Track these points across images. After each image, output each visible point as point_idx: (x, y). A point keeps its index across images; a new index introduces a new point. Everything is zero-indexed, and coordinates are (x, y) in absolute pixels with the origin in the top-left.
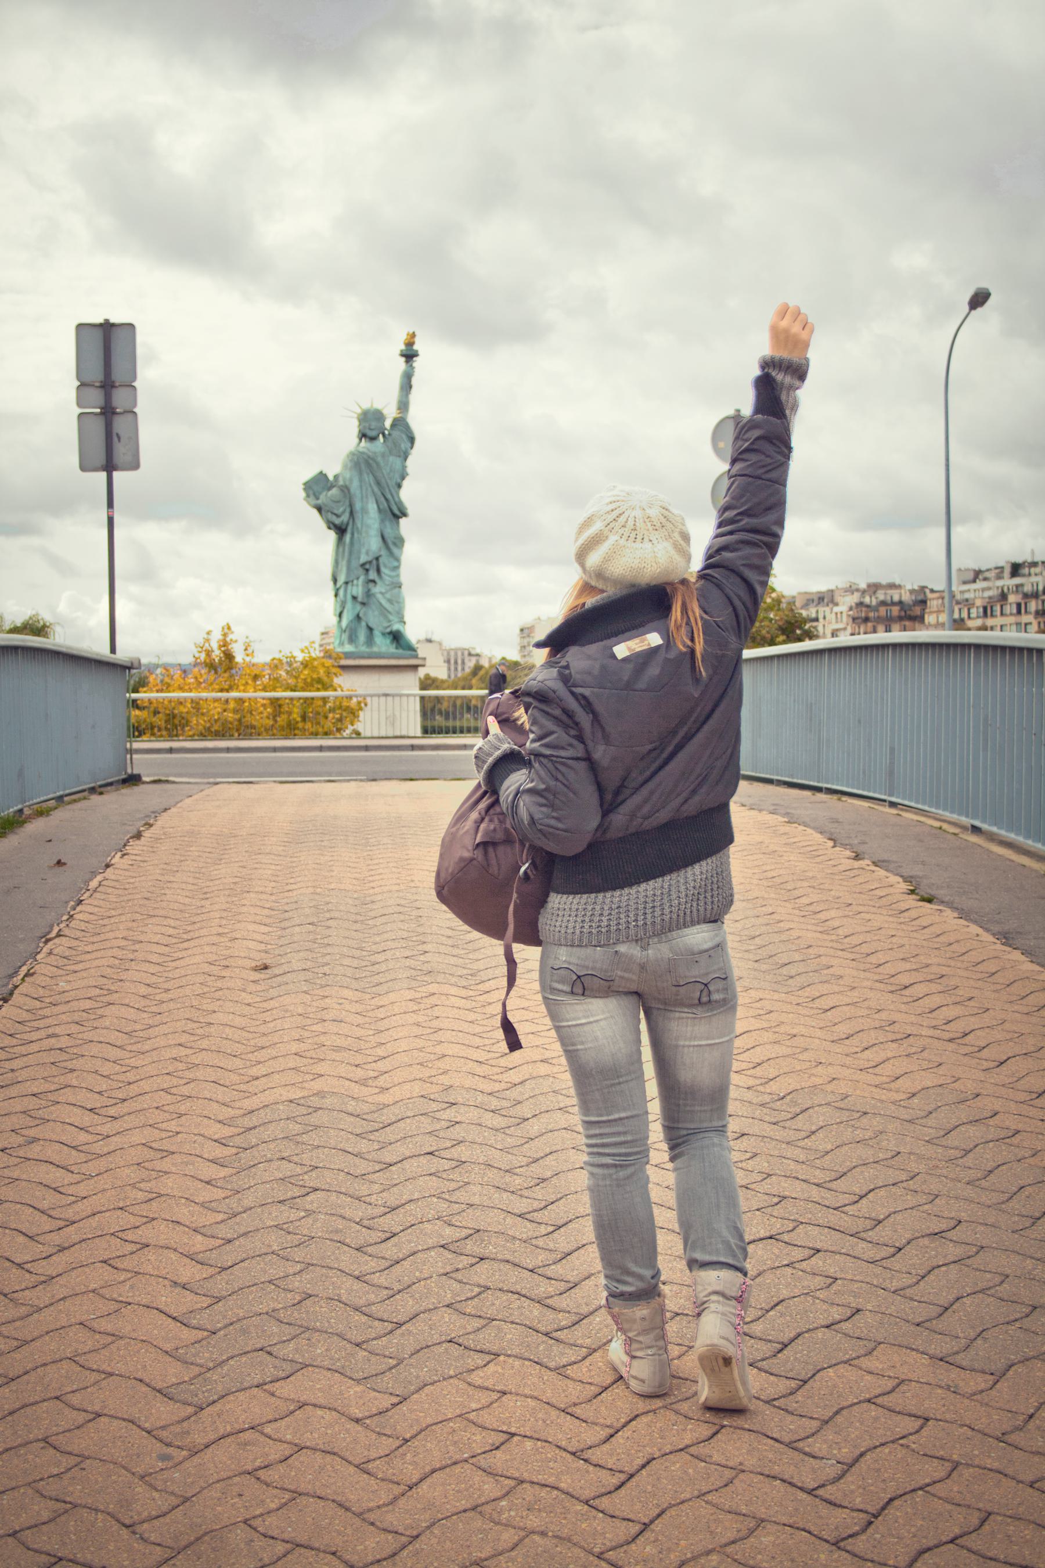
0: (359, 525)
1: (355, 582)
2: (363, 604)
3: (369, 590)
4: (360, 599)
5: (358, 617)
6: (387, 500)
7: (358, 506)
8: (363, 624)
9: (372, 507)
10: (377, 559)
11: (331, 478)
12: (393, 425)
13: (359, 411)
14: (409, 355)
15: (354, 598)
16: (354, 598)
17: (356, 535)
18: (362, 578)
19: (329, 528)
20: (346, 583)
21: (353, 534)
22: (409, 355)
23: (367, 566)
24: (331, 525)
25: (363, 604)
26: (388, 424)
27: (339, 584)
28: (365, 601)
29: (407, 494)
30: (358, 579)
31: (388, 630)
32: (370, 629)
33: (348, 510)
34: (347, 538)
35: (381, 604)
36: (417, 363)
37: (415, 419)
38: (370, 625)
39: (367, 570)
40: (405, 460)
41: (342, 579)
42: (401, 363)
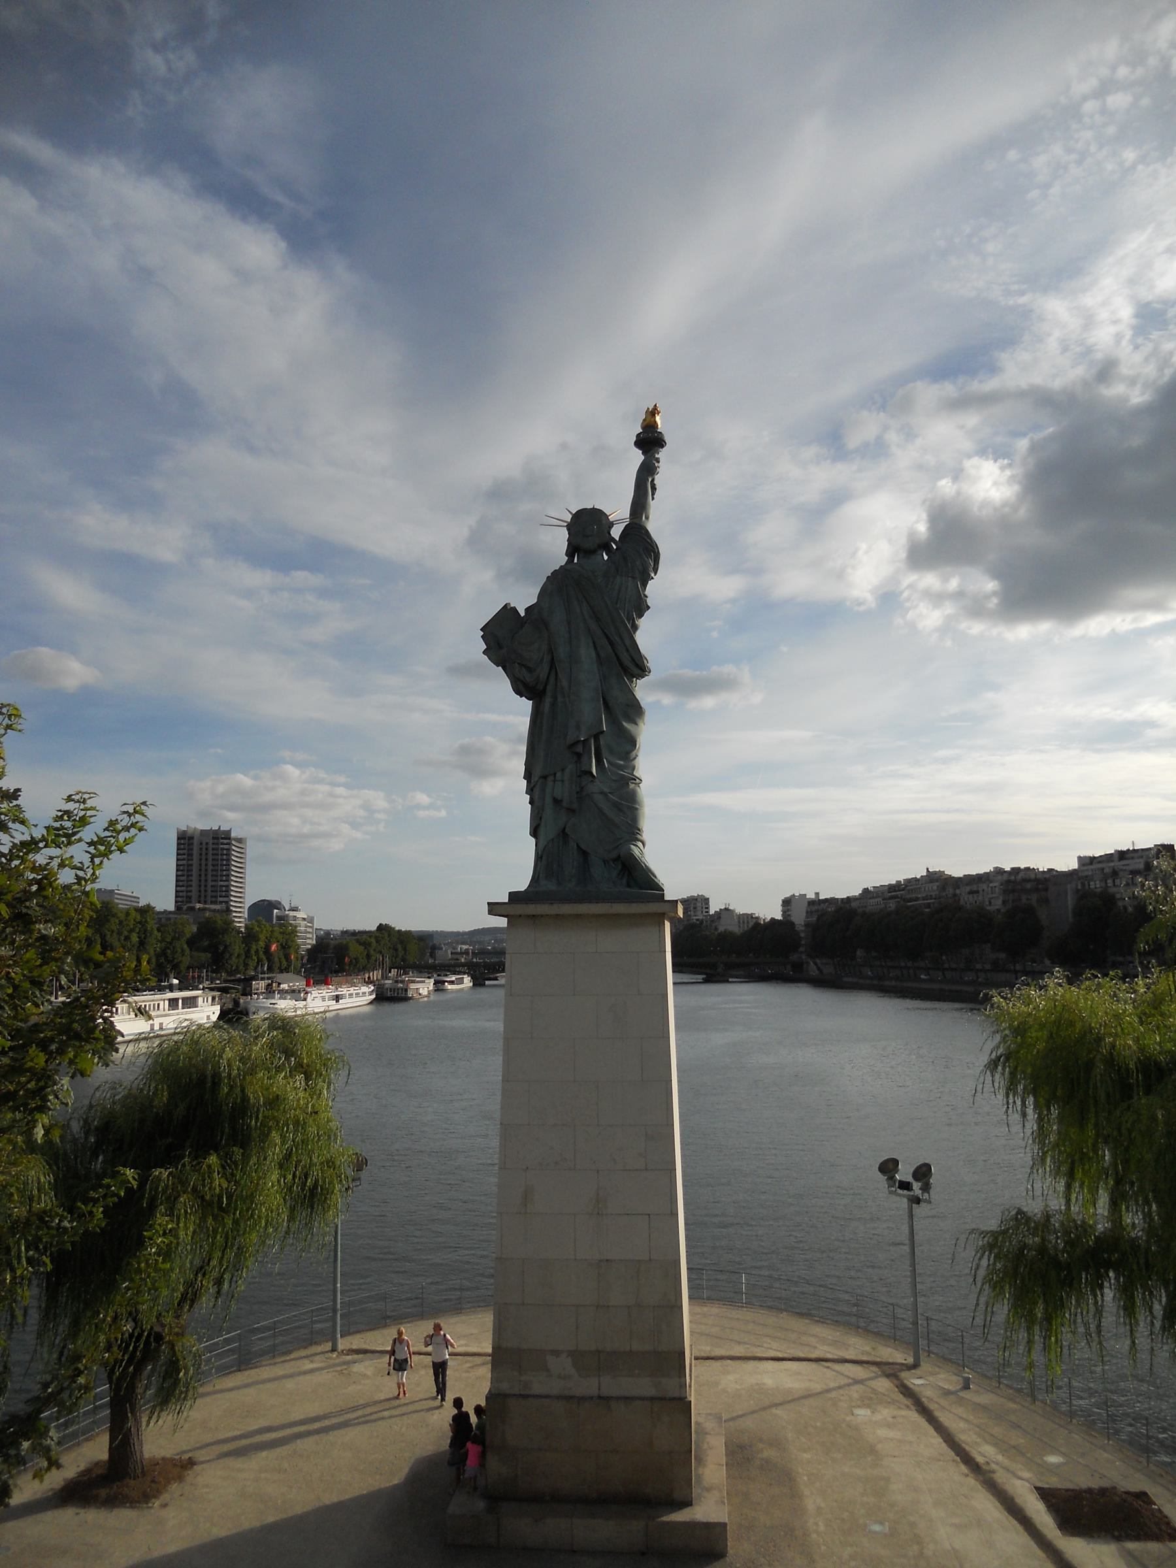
0: (565, 683)
1: (559, 775)
2: (571, 811)
3: (582, 788)
4: (565, 804)
5: (563, 834)
6: (612, 644)
7: (562, 652)
8: (572, 844)
9: (586, 654)
10: (596, 737)
11: (522, 614)
12: (624, 534)
13: (569, 518)
14: (650, 441)
15: (557, 802)
16: (557, 802)
17: (560, 699)
18: (570, 768)
19: (519, 693)
20: (545, 777)
21: (555, 698)
22: (650, 441)
23: (579, 749)
24: (521, 688)
25: (571, 811)
26: (616, 532)
27: (535, 779)
28: (575, 806)
29: (649, 636)
30: (563, 770)
31: (614, 855)
32: (584, 854)
33: (547, 659)
34: (548, 701)
35: (600, 810)
36: (662, 454)
37: (656, 524)
38: (583, 846)
39: (579, 755)
40: (645, 585)
41: (537, 772)
42: (638, 457)
